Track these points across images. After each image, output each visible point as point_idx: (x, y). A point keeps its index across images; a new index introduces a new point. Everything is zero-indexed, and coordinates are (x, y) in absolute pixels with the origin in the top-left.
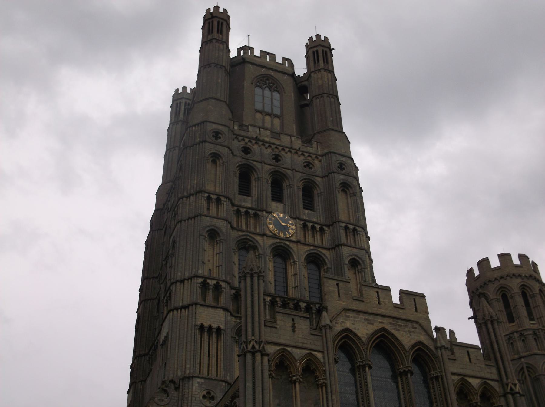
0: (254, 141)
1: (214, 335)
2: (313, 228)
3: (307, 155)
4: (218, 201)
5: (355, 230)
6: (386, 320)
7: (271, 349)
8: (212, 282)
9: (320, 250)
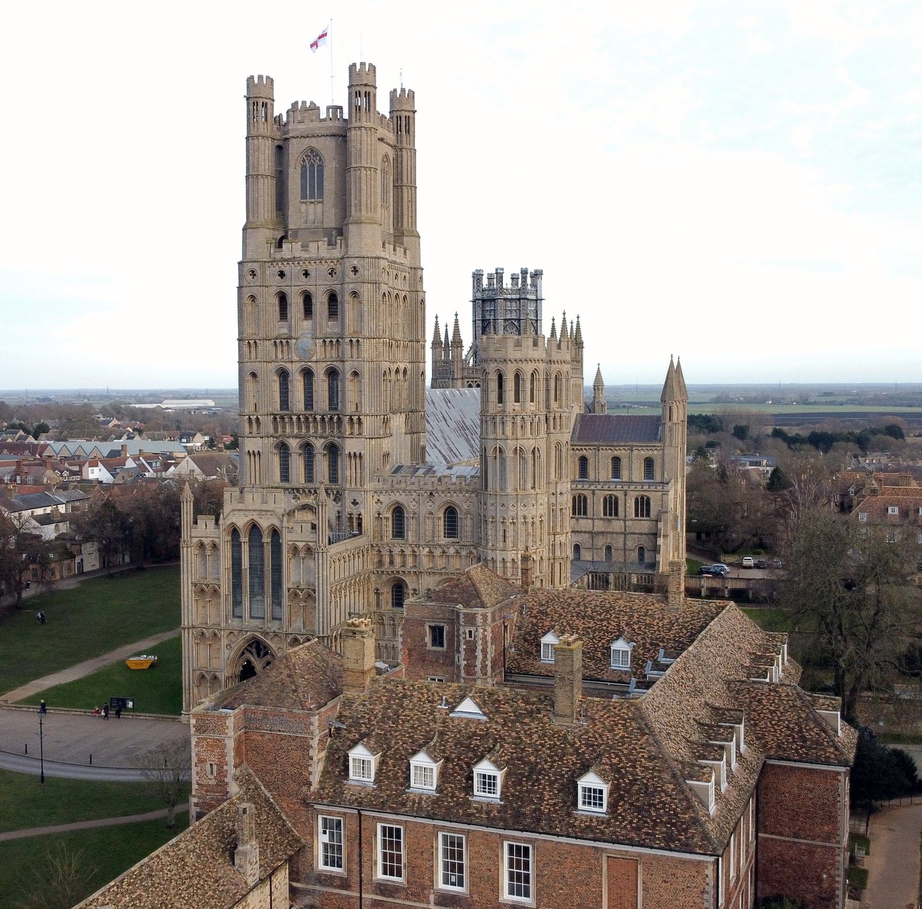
0: (285, 263)
1: (257, 457)
2: (331, 342)
3: (329, 261)
4: (255, 342)
5: (358, 341)
6: (255, 513)
7: (195, 540)
8: (253, 418)
9: (335, 363)
